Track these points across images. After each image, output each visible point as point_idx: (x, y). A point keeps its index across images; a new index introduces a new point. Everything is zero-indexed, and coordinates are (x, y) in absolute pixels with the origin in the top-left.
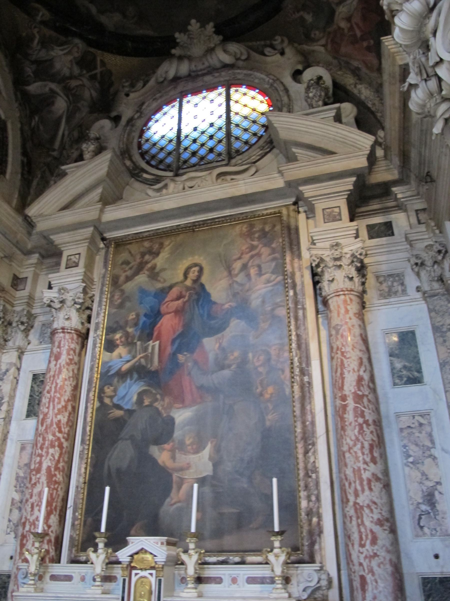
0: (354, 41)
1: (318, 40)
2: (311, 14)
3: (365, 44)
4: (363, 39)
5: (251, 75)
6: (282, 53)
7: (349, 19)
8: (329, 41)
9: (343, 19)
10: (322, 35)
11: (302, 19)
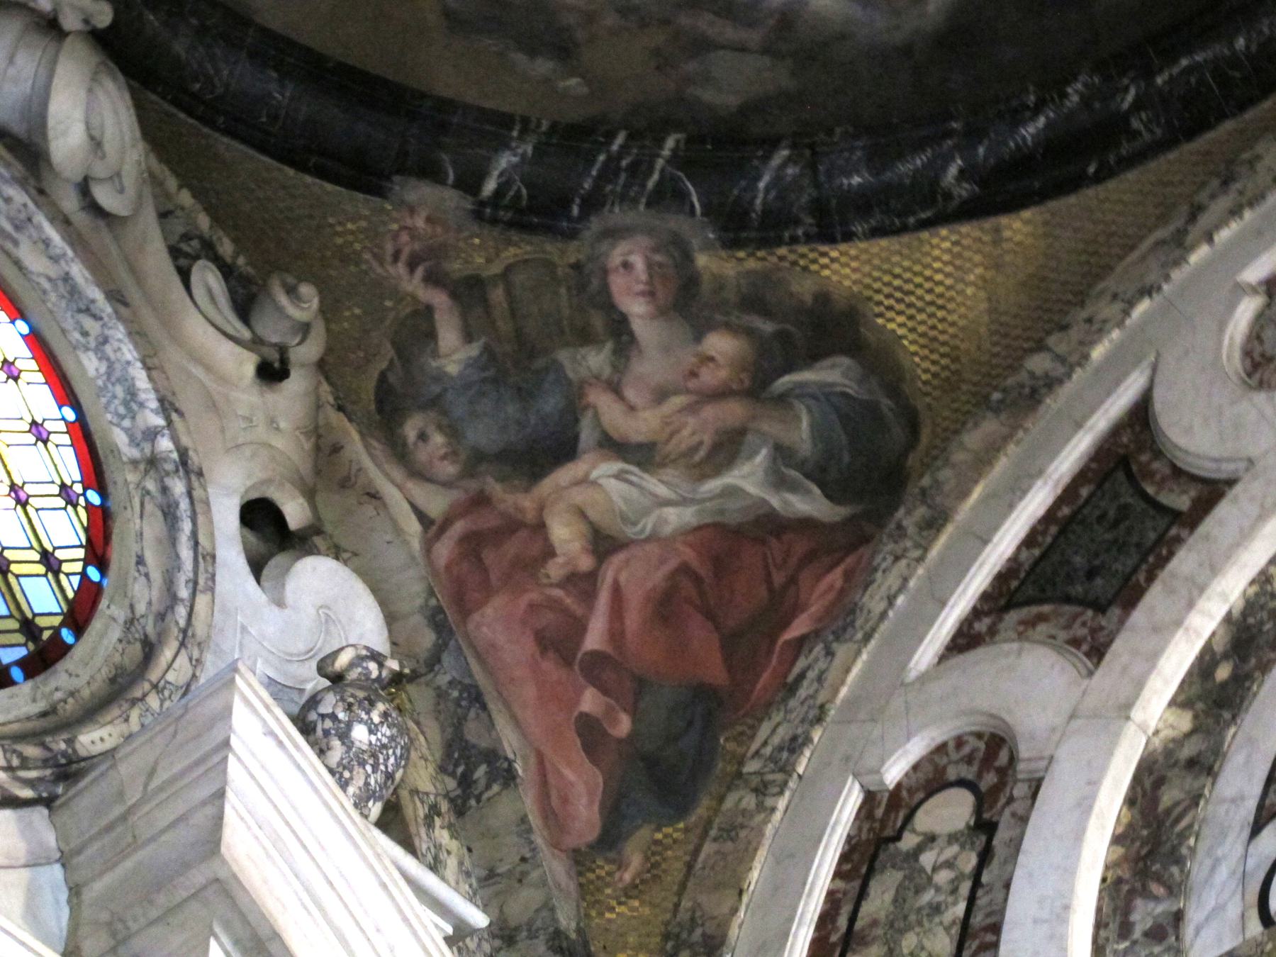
0: (559, 641)
1: (419, 474)
2: (474, 350)
3: (590, 701)
4: (596, 669)
5: (88, 310)
6: (272, 373)
7: (604, 543)
8: (459, 527)
9: (582, 514)
10: (449, 469)
11: (419, 328)
